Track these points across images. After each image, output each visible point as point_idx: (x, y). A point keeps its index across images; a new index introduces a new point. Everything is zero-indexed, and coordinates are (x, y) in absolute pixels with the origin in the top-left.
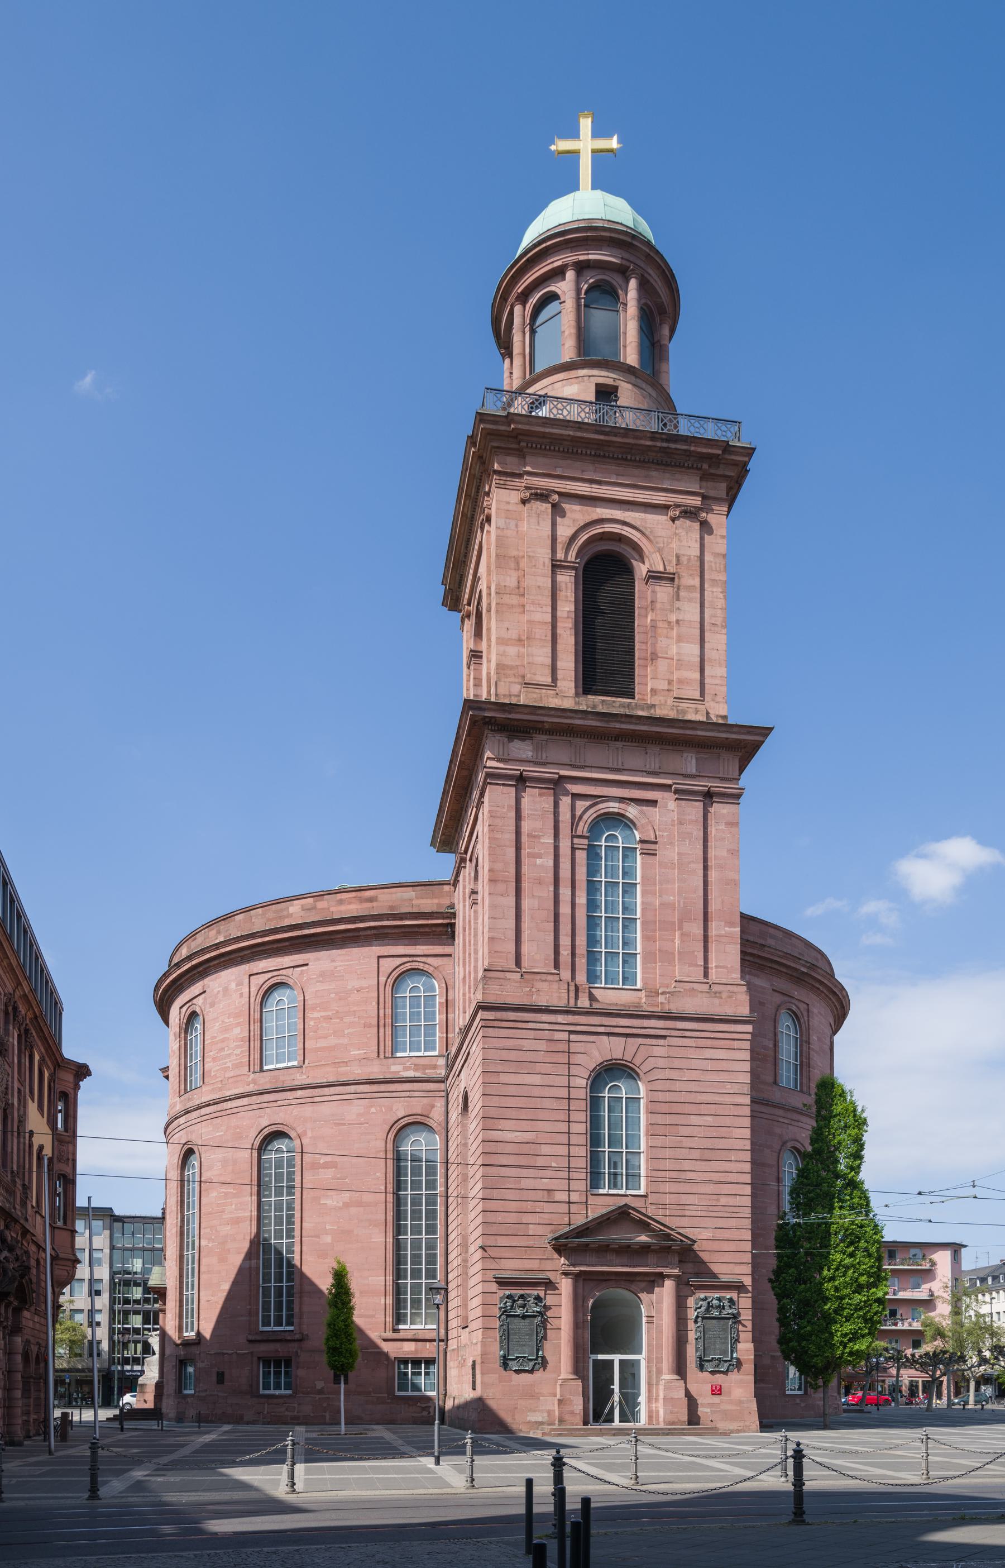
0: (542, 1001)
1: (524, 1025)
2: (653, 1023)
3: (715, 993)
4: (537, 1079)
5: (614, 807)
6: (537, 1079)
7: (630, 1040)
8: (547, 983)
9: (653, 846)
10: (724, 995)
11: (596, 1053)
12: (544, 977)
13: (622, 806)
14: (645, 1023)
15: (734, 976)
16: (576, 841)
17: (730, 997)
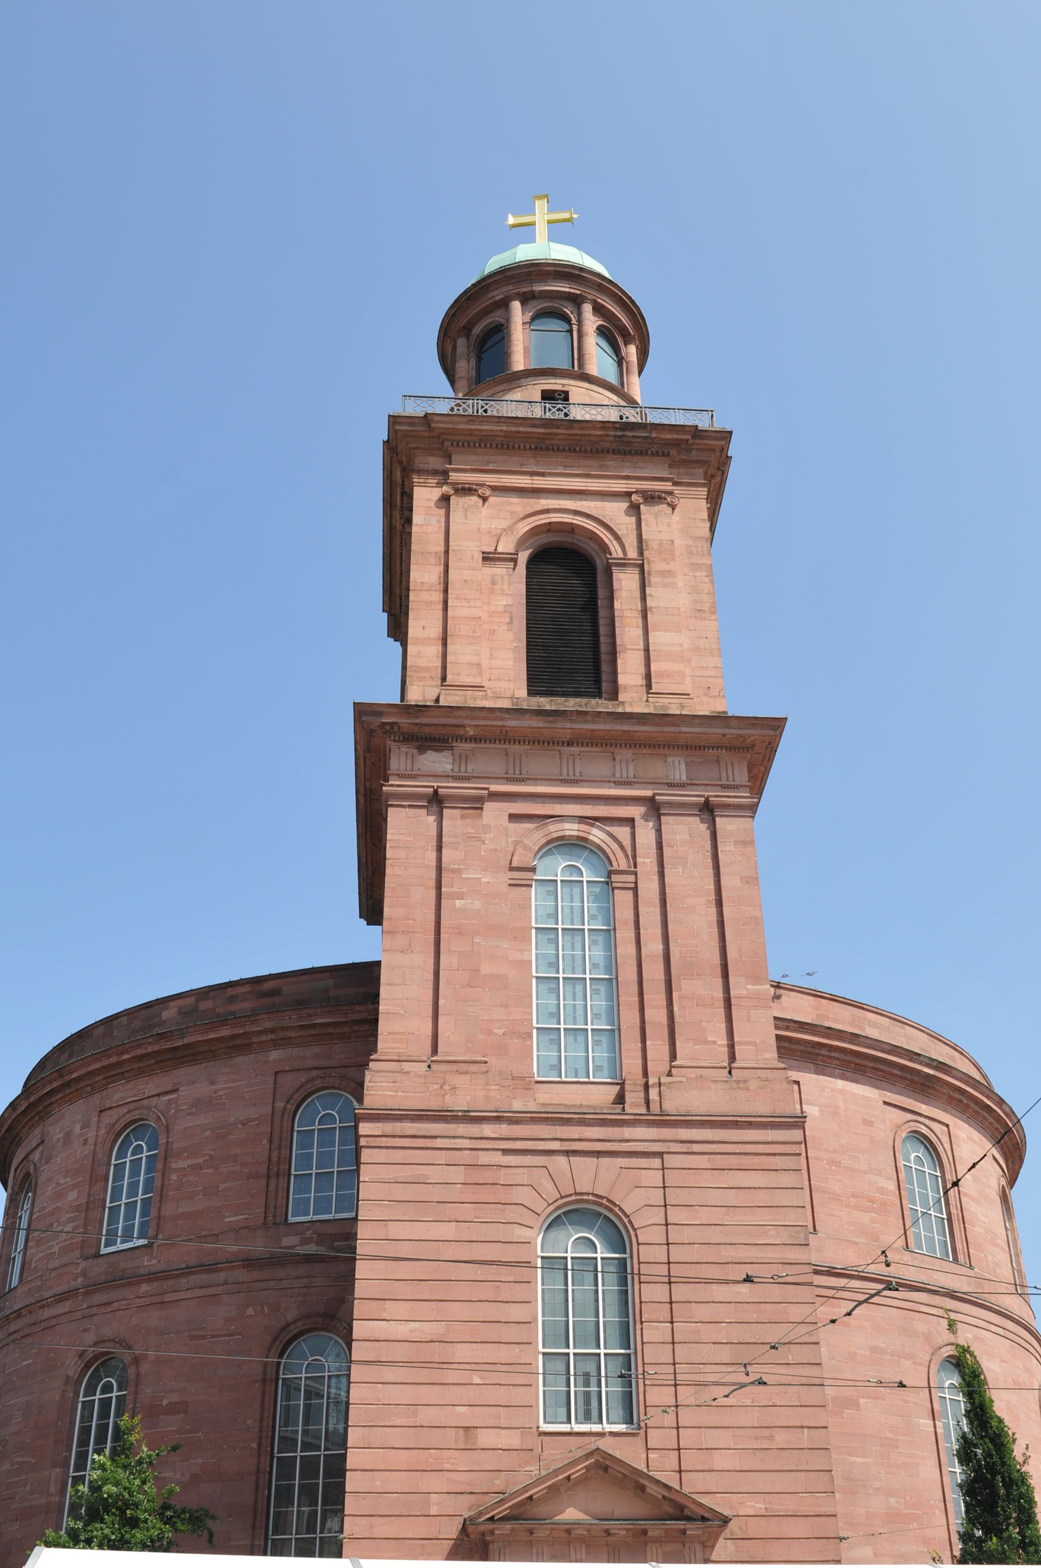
0: (459, 1102)
1: (429, 1143)
2: (640, 1132)
3: (738, 1082)
4: (448, 1230)
5: (572, 829)
6: (448, 1230)
7: (605, 1161)
8: (467, 1077)
9: (632, 878)
10: (753, 1085)
11: (549, 1185)
12: (464, 1067)
13: (583, 827)
14: (627, 1132)
15: (767, 1055)
16: (517, 874)
17: (763, 1087)
